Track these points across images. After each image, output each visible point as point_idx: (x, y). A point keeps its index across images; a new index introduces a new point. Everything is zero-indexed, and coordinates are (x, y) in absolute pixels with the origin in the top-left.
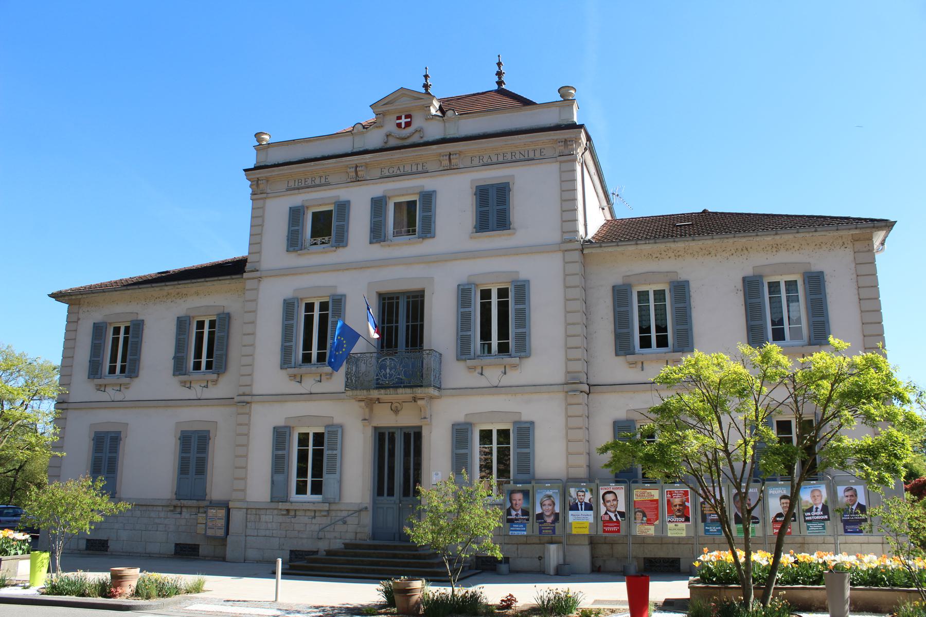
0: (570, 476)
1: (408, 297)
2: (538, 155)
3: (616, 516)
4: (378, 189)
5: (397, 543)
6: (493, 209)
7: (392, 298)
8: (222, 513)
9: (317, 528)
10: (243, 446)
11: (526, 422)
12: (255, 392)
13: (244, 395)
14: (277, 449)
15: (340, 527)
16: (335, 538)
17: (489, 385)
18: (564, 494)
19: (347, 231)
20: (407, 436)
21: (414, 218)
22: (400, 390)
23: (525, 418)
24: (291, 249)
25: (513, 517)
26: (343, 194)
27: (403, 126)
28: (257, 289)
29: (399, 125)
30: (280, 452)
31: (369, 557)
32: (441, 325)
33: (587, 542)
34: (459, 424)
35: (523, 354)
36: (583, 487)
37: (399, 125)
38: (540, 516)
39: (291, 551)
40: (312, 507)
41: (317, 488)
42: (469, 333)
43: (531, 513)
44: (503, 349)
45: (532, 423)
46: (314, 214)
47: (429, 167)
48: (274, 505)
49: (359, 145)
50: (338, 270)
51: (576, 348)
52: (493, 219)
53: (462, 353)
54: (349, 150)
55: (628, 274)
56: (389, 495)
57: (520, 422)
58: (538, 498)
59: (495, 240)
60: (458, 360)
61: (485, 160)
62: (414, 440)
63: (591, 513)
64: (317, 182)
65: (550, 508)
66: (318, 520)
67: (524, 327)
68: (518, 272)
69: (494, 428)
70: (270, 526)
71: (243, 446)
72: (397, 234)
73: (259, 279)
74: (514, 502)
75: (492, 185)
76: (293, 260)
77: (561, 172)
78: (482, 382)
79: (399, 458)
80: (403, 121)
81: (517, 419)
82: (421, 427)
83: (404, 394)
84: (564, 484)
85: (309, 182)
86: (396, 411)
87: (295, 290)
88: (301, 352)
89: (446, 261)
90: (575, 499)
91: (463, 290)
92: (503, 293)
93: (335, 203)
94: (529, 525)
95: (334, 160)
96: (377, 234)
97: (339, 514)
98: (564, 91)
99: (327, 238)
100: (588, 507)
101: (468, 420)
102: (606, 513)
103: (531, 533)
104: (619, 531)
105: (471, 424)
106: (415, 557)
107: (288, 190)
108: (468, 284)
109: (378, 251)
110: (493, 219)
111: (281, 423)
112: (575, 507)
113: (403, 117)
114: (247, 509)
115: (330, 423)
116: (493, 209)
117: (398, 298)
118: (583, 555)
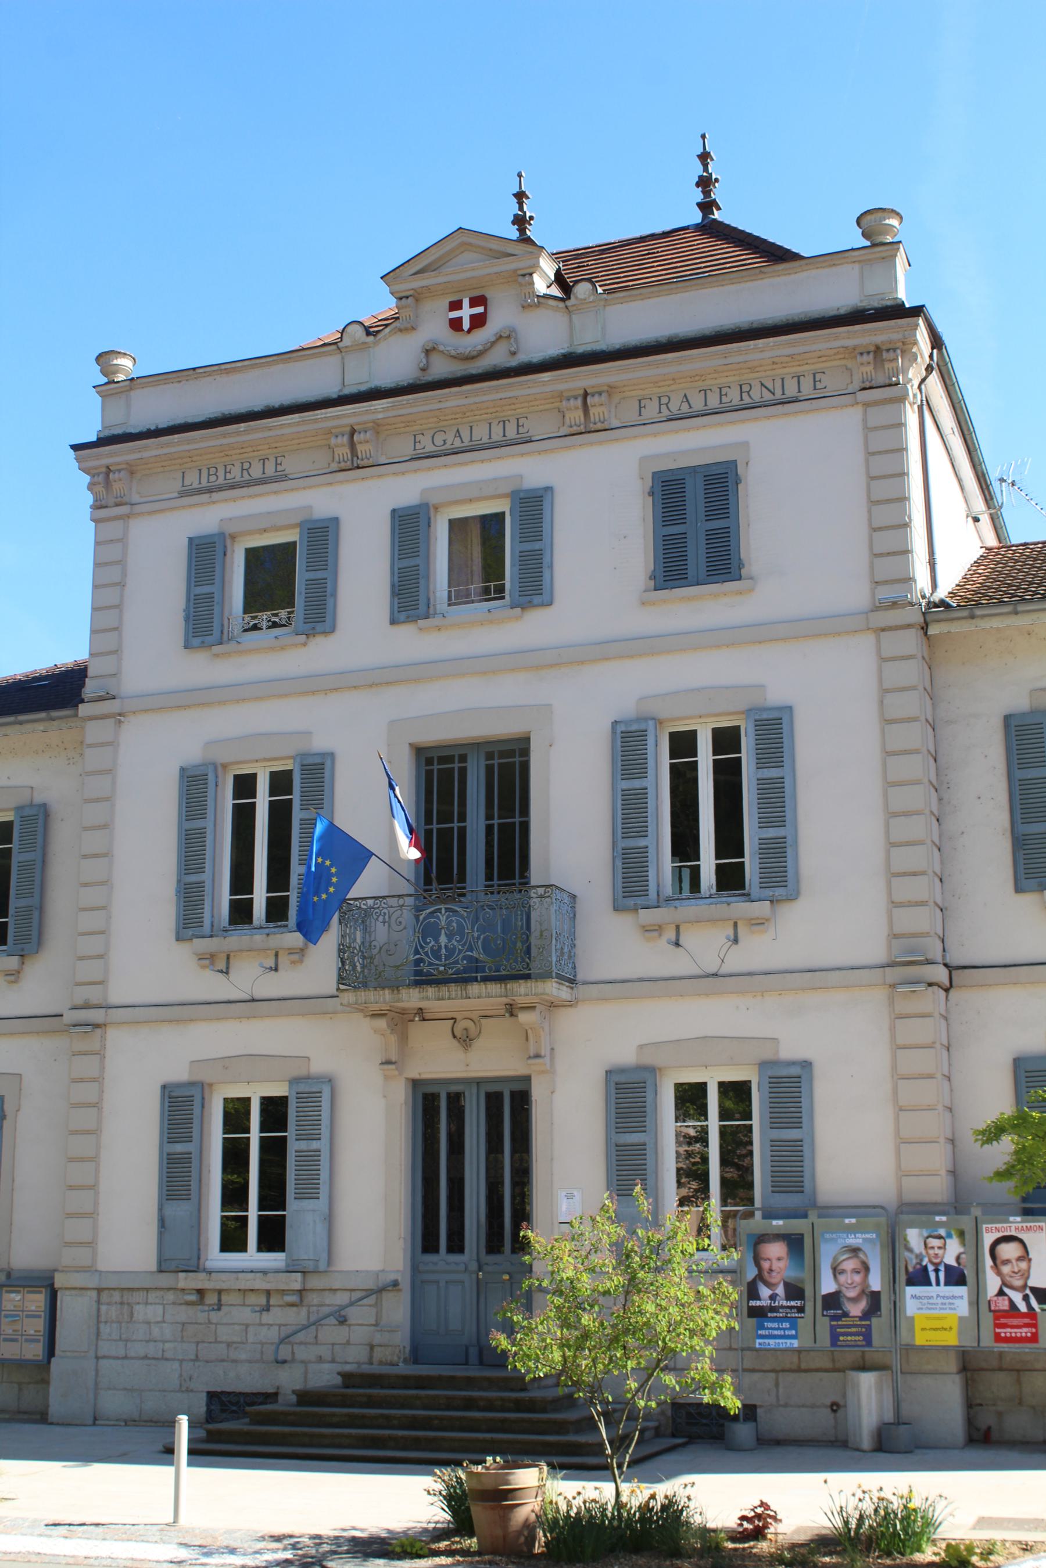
0: (908, 1197)
1: (490, 756)
2: (807, 389)
3: (1026, 1298)
4: (406, 488)
5: (474, 1372)
6: (697, 530)
7: (449, 759)
8: (37, 1301)
9: (273, 1334)
10: (88, 1132)
12: (114, 999)
13: (87, 1006)
14: (172, 1141)
15: (331, 1333)
16: (320, 1360)
18: (893, 1243)
19: (334, 595)
20: (493, 1100)
21: (498, 557)
22: (474, 989)
23: (787, 1052)
24: (196, 641)
25: (765, 1302)
26: (321, 500)
27: (466, 325)
28: (112, 744)
29: (456, 324)
30: (179, 1148)
31: (403, 1407)
32: (572, 825)
34: (622, 1070)
35: (779, 892)
36: (941, 1224)
37: (456, 324)
38: (833, 1301)
39: (212, 1396)
40: (260, 1283)
41: (273, 1237)
42: (642, 842)
43: (809, 1293)
44: (730, 879)
46: (248, 551)
47: (536, 427)
48: (165, 1280)
49: (358, 379)
50: (314, 693)
51: (914, 874)
52: (697, 556)
53: (628, 894)
54: (332, 390)
56: (450, 1250)
58: (827, 1253)
60: (616, 909)
61: (674, 406)
62: (510, 1110)
63: (961, 1291)
64: (256, 472)
65: (857, 1278)
66: (277, 1315)
67: (782, 824)
68: (762, 687)
69: (712, 1078)
70: (156, 1331)
71: (88, 1132)
72: (458, 597)
73: (119, 717)
74: (766, 1265)
75: (694, 470)
77: (868, 429)
78: (678, 964)
79: (472, 1160)
80: (466, 313)
81: (768, 1056)
82: (527, 1079)
83: (485, 996)
84: (891, 1220)
85: (236, 473)
86: (466, 1040)
87: (208, 744)
88: (225, 897)
89: (582, 662)
90: (920, 1257)
91: (626, 736)
92: (726, 740)
93: (301, 525)
94: (805, 1322)
95: (295, 417)
96: (408, 600)
99: (283, 613)
100: (955, 1277)
101: (648, 1060)
102: (1001, 1293)
103: (809, 1343)
104: (1034, 1338)
106: (519, 1406)
107: (184, 493)
109: (412, 643)
110: (697, 556)
111: (179, 1073)
112: (920, 1277)
113: (466, 303)
114: (99, 1290)
115: (303, 1072)
116: (697, 530)
117: (463, 758)
118: (944, 1400)
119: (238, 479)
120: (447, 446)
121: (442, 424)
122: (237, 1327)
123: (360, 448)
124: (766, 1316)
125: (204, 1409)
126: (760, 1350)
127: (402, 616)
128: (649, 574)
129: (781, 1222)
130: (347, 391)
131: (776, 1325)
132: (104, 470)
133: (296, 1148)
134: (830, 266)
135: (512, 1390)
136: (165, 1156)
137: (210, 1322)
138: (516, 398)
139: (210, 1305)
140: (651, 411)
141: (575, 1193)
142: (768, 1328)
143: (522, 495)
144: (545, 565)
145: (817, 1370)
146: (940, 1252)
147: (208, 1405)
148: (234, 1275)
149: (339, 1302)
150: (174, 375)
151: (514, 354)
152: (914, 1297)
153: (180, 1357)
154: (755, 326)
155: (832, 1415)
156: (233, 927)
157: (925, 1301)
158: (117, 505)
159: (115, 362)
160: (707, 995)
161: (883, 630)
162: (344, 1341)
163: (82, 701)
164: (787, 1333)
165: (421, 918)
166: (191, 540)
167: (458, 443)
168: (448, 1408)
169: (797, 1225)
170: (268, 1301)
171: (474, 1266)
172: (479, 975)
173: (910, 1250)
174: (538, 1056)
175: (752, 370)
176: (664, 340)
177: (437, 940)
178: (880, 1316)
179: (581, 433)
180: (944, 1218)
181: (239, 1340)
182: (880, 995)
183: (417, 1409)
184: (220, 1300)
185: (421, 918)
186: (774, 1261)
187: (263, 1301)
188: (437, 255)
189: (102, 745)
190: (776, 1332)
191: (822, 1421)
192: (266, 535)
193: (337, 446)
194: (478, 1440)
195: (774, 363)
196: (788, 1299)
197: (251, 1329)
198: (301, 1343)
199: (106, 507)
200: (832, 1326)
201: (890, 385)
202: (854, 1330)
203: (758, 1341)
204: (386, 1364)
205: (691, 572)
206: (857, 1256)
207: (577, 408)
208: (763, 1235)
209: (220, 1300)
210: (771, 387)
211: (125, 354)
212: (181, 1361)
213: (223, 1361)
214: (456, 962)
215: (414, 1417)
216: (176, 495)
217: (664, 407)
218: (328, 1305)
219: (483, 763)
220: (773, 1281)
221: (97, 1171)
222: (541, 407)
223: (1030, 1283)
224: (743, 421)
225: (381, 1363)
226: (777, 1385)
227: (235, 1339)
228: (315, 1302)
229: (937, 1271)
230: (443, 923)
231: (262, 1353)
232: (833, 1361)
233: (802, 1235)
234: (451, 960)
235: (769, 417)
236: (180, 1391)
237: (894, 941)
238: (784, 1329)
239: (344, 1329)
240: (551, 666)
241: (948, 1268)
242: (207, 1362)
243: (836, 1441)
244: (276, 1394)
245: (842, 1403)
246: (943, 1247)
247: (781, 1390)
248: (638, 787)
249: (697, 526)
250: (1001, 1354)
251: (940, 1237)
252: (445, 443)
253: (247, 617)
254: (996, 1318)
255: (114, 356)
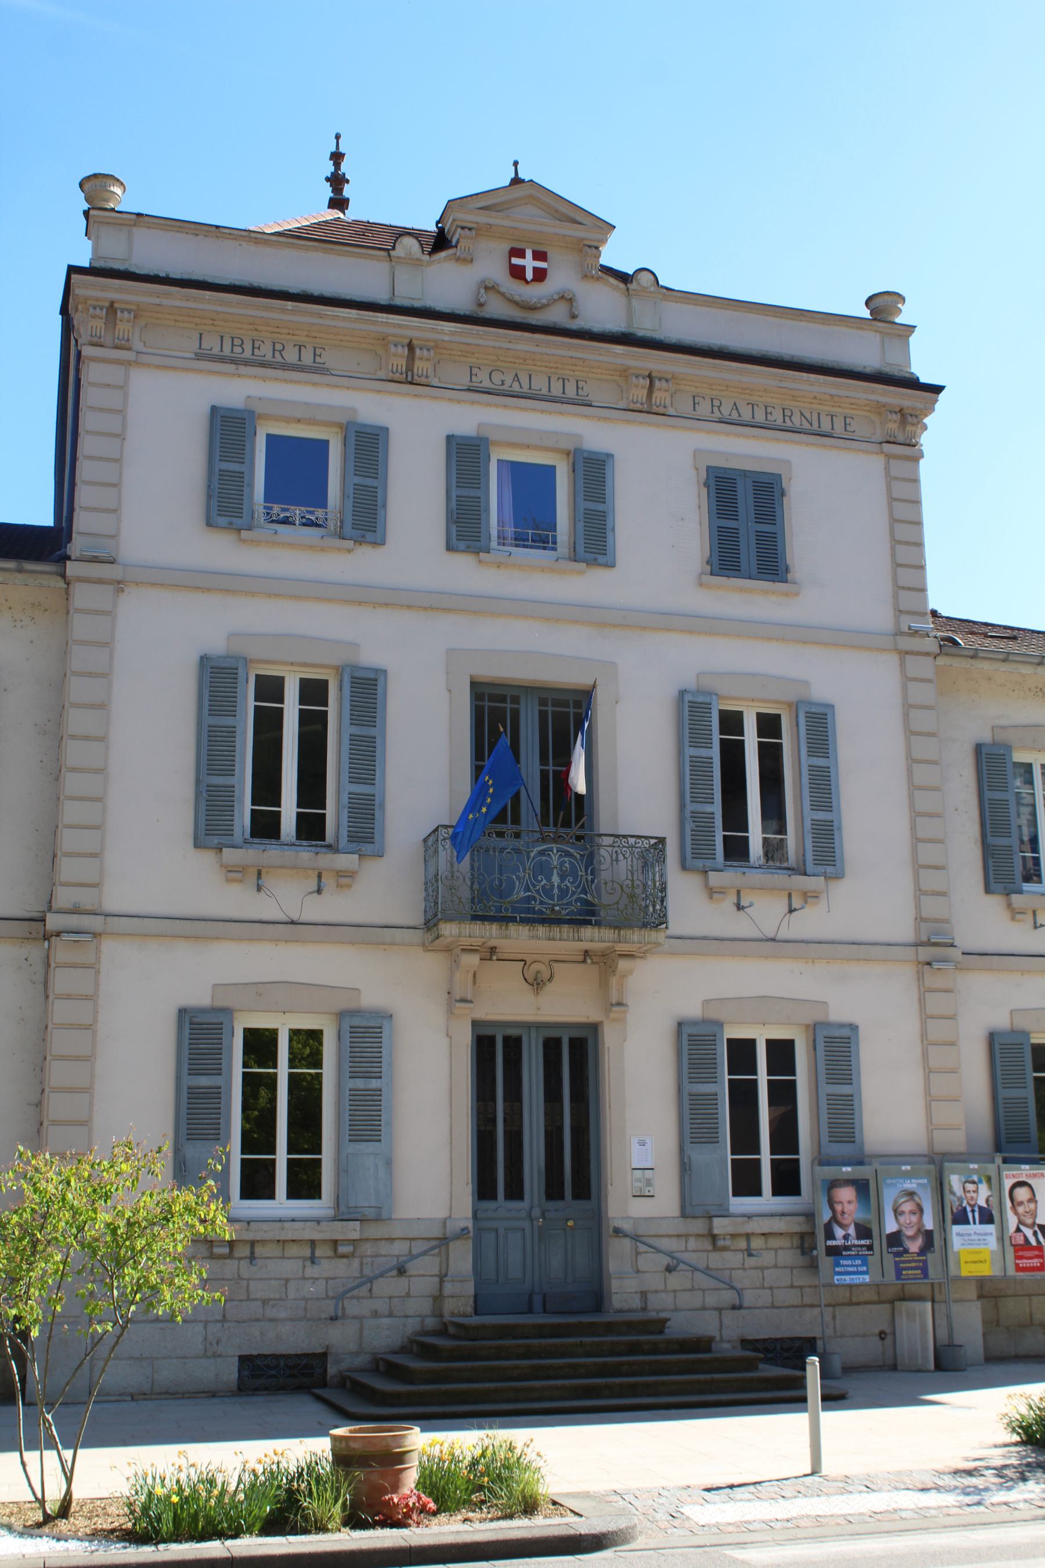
0: (939, 1148)
1: (543, 702)
2: (839, 428)
3: (1035, 1234)
4: (468, 418)
6: (747, 529)
7: (503, 699)
10: (78, 1058)
11: (841, 1026)
12: (109, 906)
13: (76, 911)
15: (389, 1286)
16: (375, 1314)
17: (760, 936)
18: (940, 1187)
19: (384, 506)
20: (552, 1047)
23: (837, 1015)
24: (223, 521)
25: (839, 1242)
26: (372, 407)
27: (529, 275)
28: (109, 614)
29: (517, 273)
30: (204, 1081)
31: (563, 1355)
33: (972, 1293)
34: (694, 1023)
35: (830, 870)
36: (975, 1171)
37: (517, 273)
38: (895, 1239)
39: (244, 1360)
41: (305, 1183)
45: (854, 1028)
50: (360, 603)
54: (383, 298)
55: (1003, 722)
56: (576, 1196)
57: (828, 1025)
58: (889, 1196)
59: (746, 600)
61: (726, 410)
63: (990, 1228)
64: (291, 356)
65: (914, 1219)
69: (761, 1035)
71: (78, 1058)
73: (119, 585)
74: (839, 1208)
75: (745, 473)
76: (221, 551)
77: (890, 479)
78: (740, 926)
80: (529, 263)
81: (819, 1017)
82: (594, 1028)
83: (566, 942)
85: (265, 351)
86: (537, 984)
87: (231, 636)
89: (644, 628)
90: (960, 1199)
91: (693, 705)
94: (874, 1260)
95: (353, 313)
96: (464, 529)
97: (384, 1248)
98: (883, 307)
99: (320, 513)
100: (986, 1217)
101: (713, 1014)
102: (1018, 1230)
103: (878, 1279)
105: (720, 1025)
107: (199, 357)
108: (699, 692)
109: (465, 573)
111: (200, 997)
112: (961, 1218)
113: (529, 254)
115: (352, 1005)
116: (747, 529)
117: (516, 700)
118: (969, 1323)
119: (269, 357)
120: (506, 387)
121: (499, 363)
122: (273, 1282)
123: (419, 365)
124: (841, 1254)
125: (235, 1376)
126: (837, 1286)
127: (462, 545)
128: (706, 559)
129: (849, 1169)
130: (398, 302)
131: (849, 1262)
132: (107, 304)
133: (351, 1086)
134: (858, 328)
135: (651, 1333)
136: (185, 1090)
137: (240, 1277)
138: (584, 360)
139: (240, 1259)
140: (704, 408)
141: (648, 1140)
142: (844, 1266)
143: (585, 455)
144: (609, 527)
145: (866, 1303)
146: (974, 1195)
147: (239, 1371)
148: (279, 1224)
149: (396, 1252)
150: (192, 226)
151: (574, 317)
152: (958, 1234)
153: (203, 1318)
154: (795, 360)
155: (881, 1342)
156: (298, 842)
157: (966, 1238)
158: (116, 347)
159: (112, 189)
160: (766, 958)
161: (907, 653)
162: (404, 1294)
163: (69, 558)
164: (860, 1269)
165: (532, 854)
166: (214, 409)
167: (516, 387)
168: (612, 1353)
169: (863, 1172)
170: (313, 1252)
171: (536, 1212)
172: (593, 919)
173: (953, 1193)
174: (619, 1004)
175: (794, 398)
176: (716, 348)
177: (549, 879)
178: (934, 1252)
179: (640, 411)
180: (976, 1166)
181: (278, 1296)
182: (908, 971)
183: (578, 1356)
184: (252, 1253)
185: (532, 854)
186: (846, 1204)
187: (307, 1252)
188: (504, 199)
189: (97, 612)
190: (850, 1269)
191: (871, 1349)
192: (294, 425)
193: (395, 355)
194: (698, 1381)
195: (815, 398)
196: (859, 1238)
197: (292, 1285)
198: (353, 1297)
199: (102, 346)
200: (896, 1262)
201: (909, 445)
202: (913, 1264)
203: (836, 1277)
204: (459, 1315)
205: (744, 565)
206: (913, 1199)
207: (643, 387)
208: (835, 1180)
209: (252, 1253)
210: (809, 418)
211: (122, 184)
212: (206, 1323)
213: (258, 1320)
214: (569, 904)
215: (605, 1364)
216: (193, 356)
217: (716, 409)
218: (385, 1256)
219: (537, 708)
220: (845, 1222)
221: (91, 1105)
222: (599, 376)
223: (1039, 1221)
224: (786, 441)
225: (453, 1314)
226: (834, 1318)
227: (272, 1296)
228: (369, 1252)
229: (973, 1211)
230: (555, 863)
231: (306, 1309)
232: (879, 1293)
233: (868, 1180)
234: (565, 901)
235: (808, 444)
236: (205, 1356)
237: (922, 924)
238: (857, 1266)
239: (403, 1282)
240: (615, 626)
241: (981, 1208)
242: (238, 1322)
243: (884, 1366)
244: (324, 1355)
245: (888, 1331)
246: (976, 1191)
247: (838, 1322)
248: (704, 755)
249: (747, 527)
250: (1022, 1281)
251: (974, 1182)
252: (503, 384)
253: (276, 508)
254: (1016, 1251)
255: (110, 181)
